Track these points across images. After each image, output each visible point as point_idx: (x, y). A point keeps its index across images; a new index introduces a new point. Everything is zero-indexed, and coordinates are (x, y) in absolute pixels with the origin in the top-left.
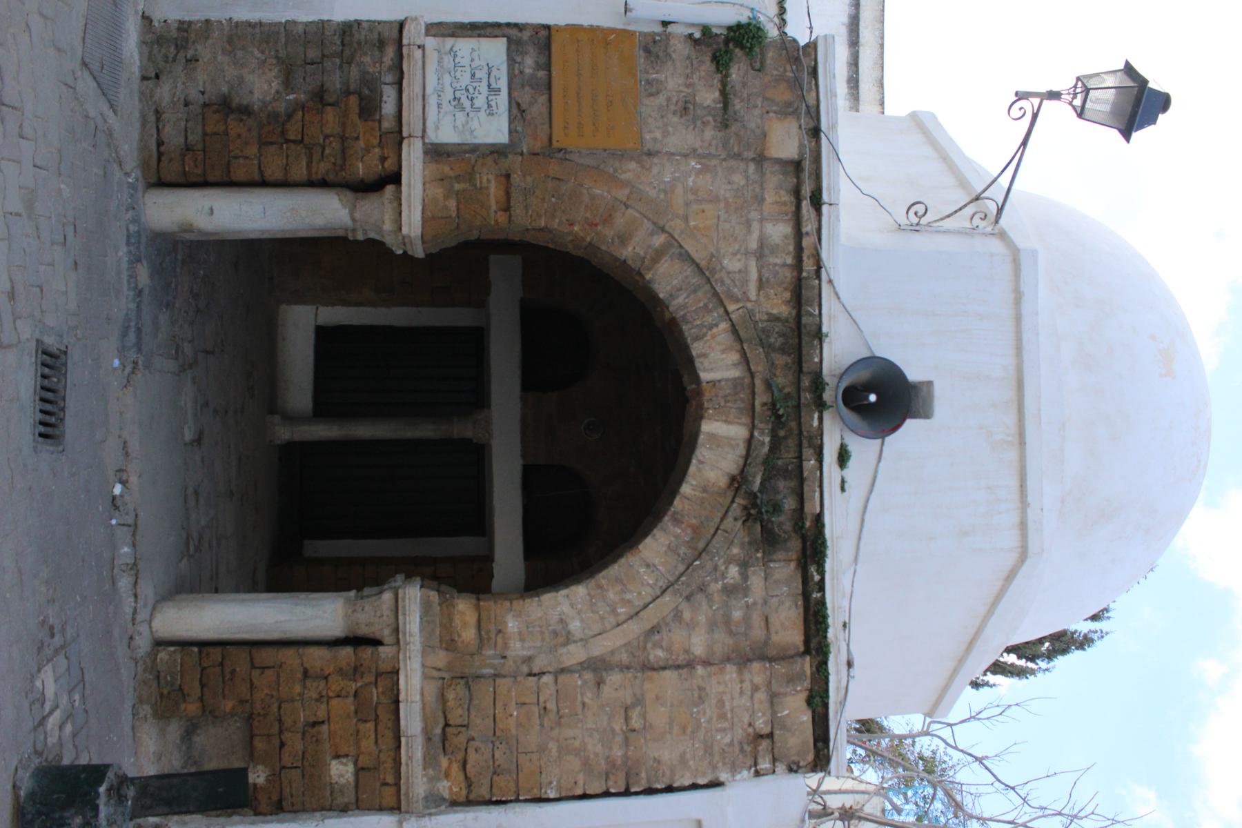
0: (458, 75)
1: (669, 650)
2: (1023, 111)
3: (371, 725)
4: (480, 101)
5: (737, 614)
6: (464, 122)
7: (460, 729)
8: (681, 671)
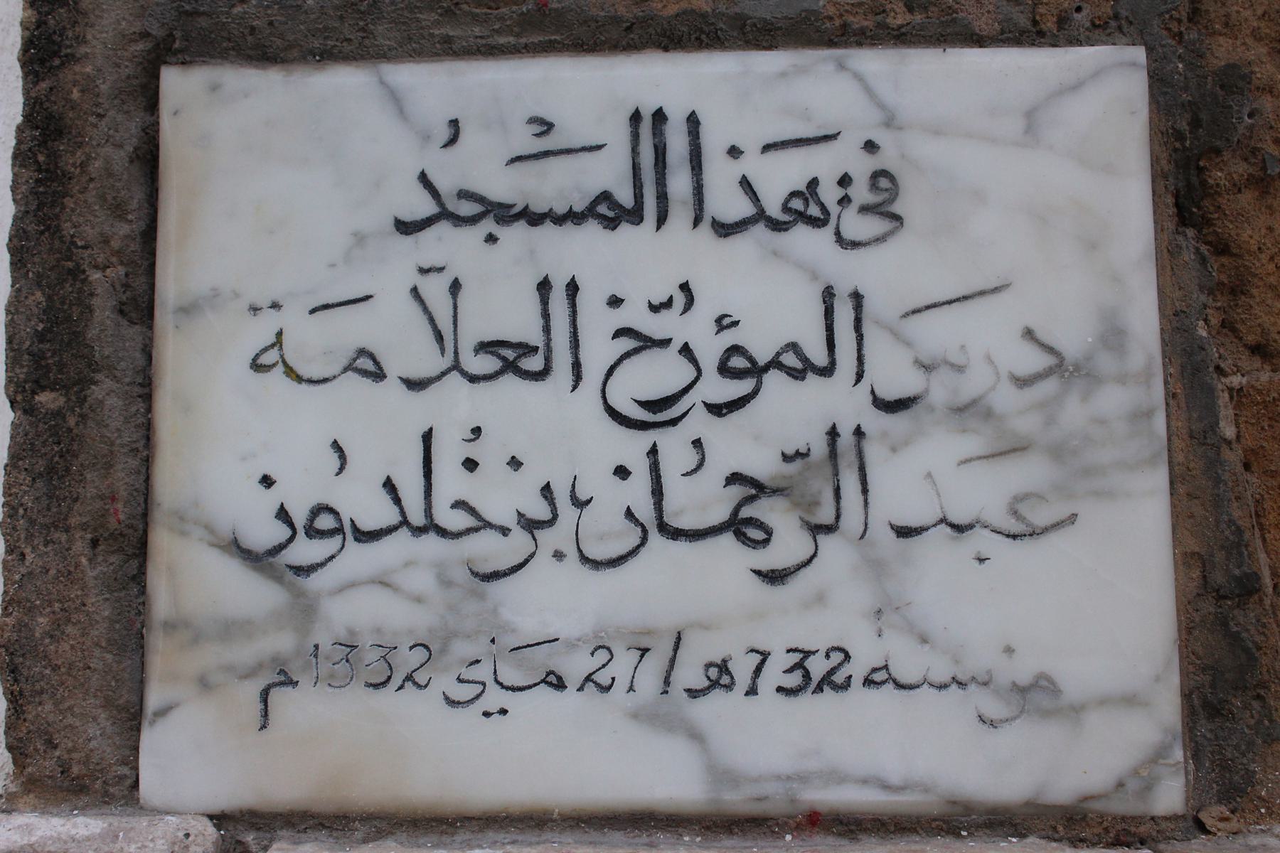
6: (972, 444)
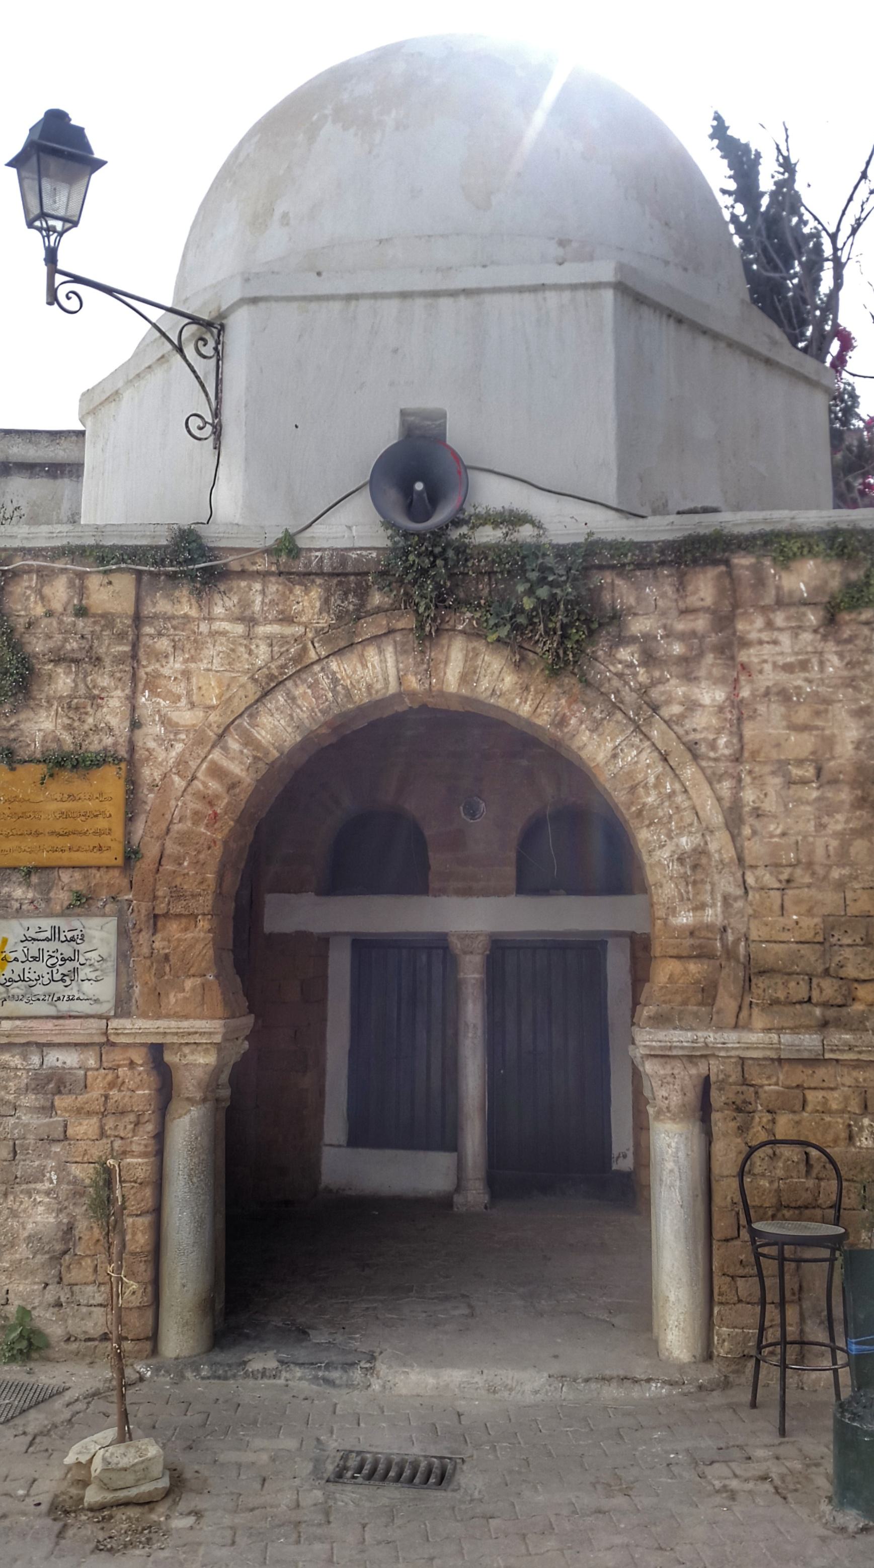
0: (35, 976)
1: (719, 731)
2: (70, 295)
3: (811, 1096)
4: (67, 950)
5: (677, 649)
7: (814, 985)
8: (745, 716)
